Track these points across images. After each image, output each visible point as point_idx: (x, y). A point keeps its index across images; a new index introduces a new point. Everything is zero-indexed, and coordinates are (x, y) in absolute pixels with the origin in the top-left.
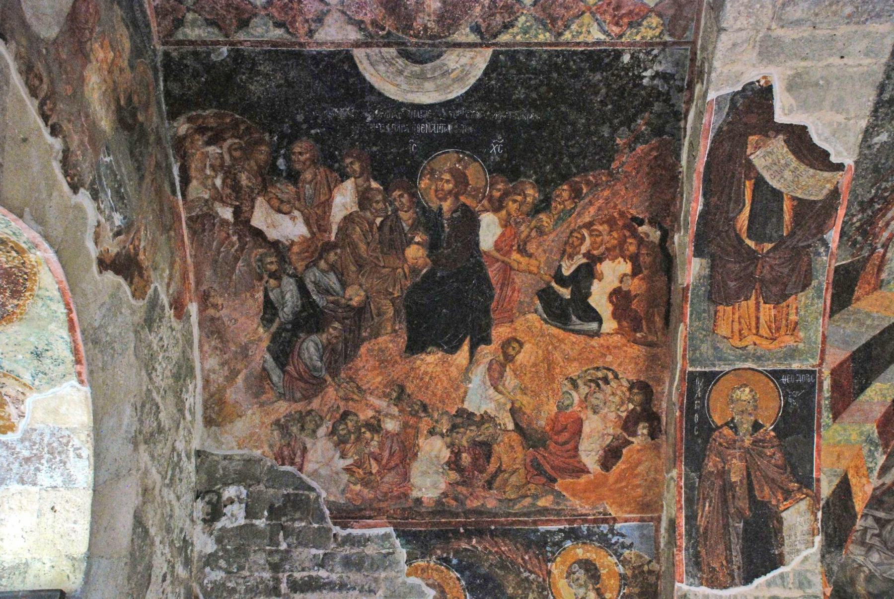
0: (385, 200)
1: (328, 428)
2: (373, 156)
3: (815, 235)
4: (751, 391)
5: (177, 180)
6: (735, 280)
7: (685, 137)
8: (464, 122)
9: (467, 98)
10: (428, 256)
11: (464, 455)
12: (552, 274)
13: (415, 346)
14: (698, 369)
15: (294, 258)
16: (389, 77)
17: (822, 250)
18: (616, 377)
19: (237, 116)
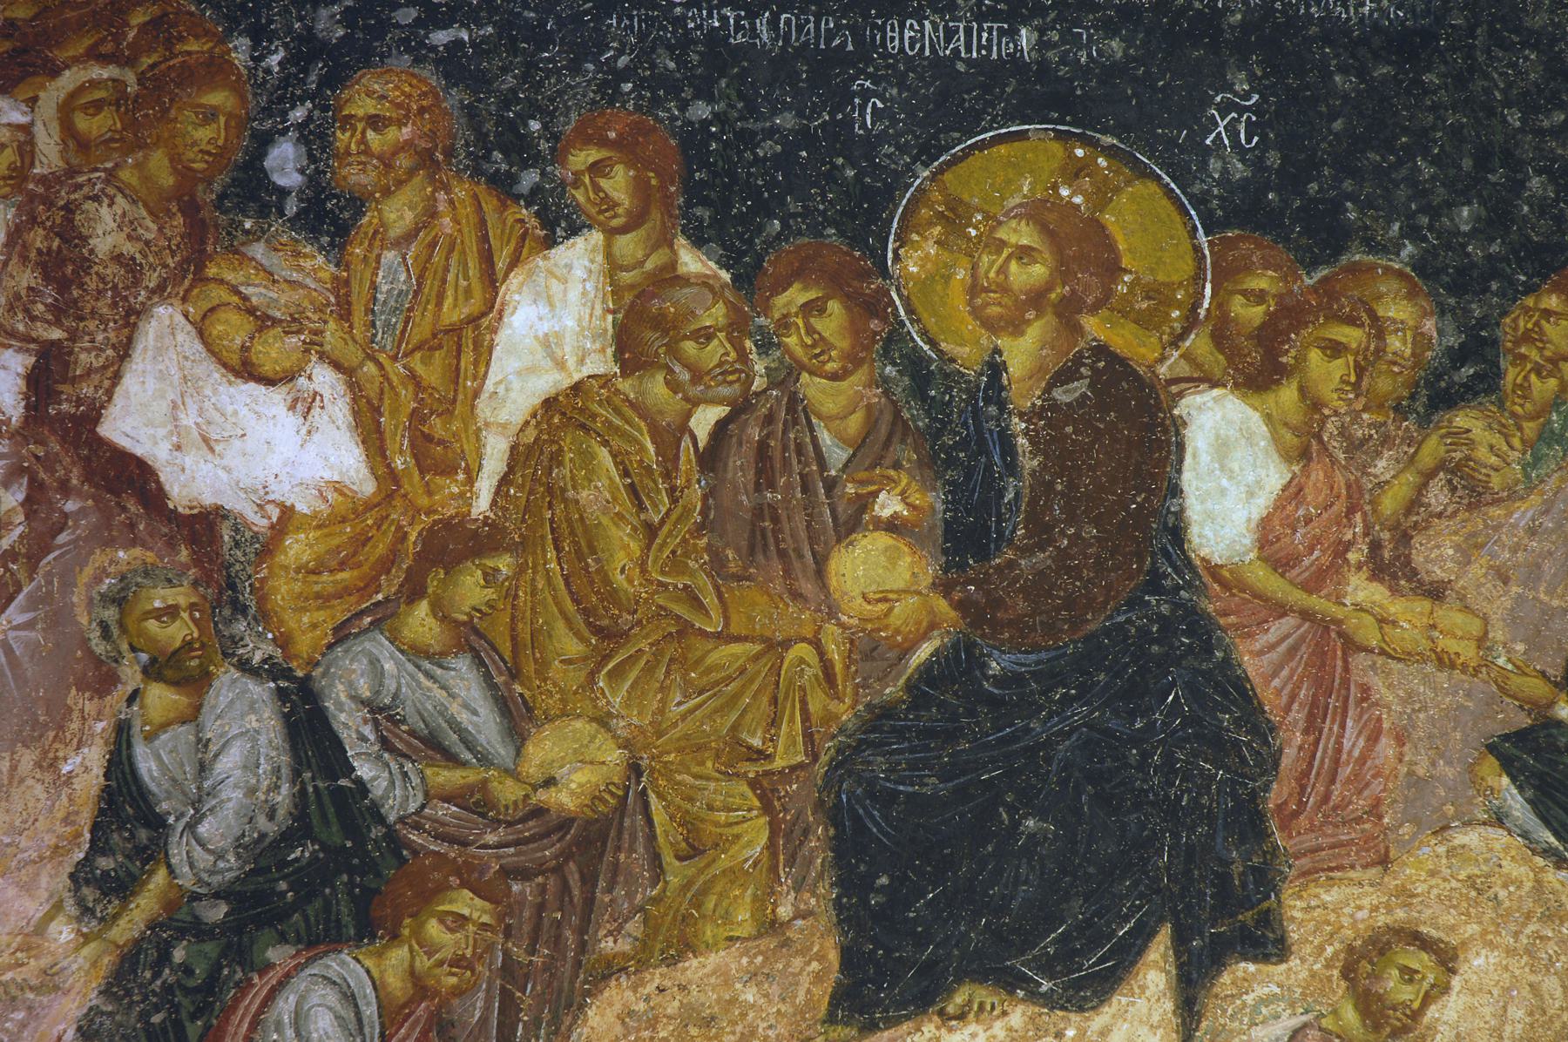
0: (737, 327)
2: (693, 140)
10: (944, 587)
15: (283, 591)
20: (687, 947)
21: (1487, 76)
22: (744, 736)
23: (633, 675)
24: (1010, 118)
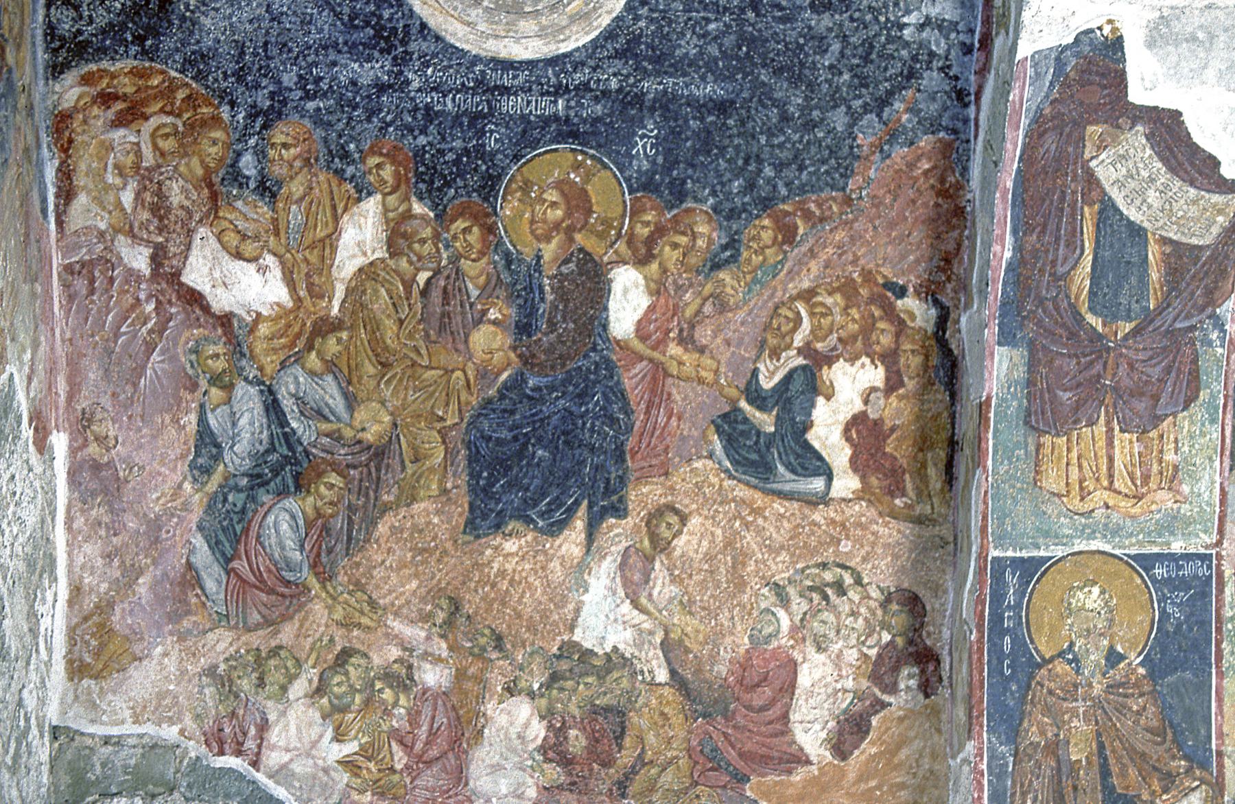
0: (437, 236)
1: (310, 681)
2: (419, 153)
3: (1202, 309)
4: (1103, 592)
5: (51, 192)
6: (1071, 389)
7: (976, 137)
8: (588, 95)
9: (594, 53)
10: (514, 348)
11: (573, 733)
12: (742, 387)
13: (485, 517)
14: (1010, 553)
15: (259, 347)
16: (455, 9)
17: (1214, 336)
18: (858, 582)
19: (173, 74)
20: (414, 499)
21: (754, 121)
22: (436, 410)
23: (394, 383)
24: (552, 142)
